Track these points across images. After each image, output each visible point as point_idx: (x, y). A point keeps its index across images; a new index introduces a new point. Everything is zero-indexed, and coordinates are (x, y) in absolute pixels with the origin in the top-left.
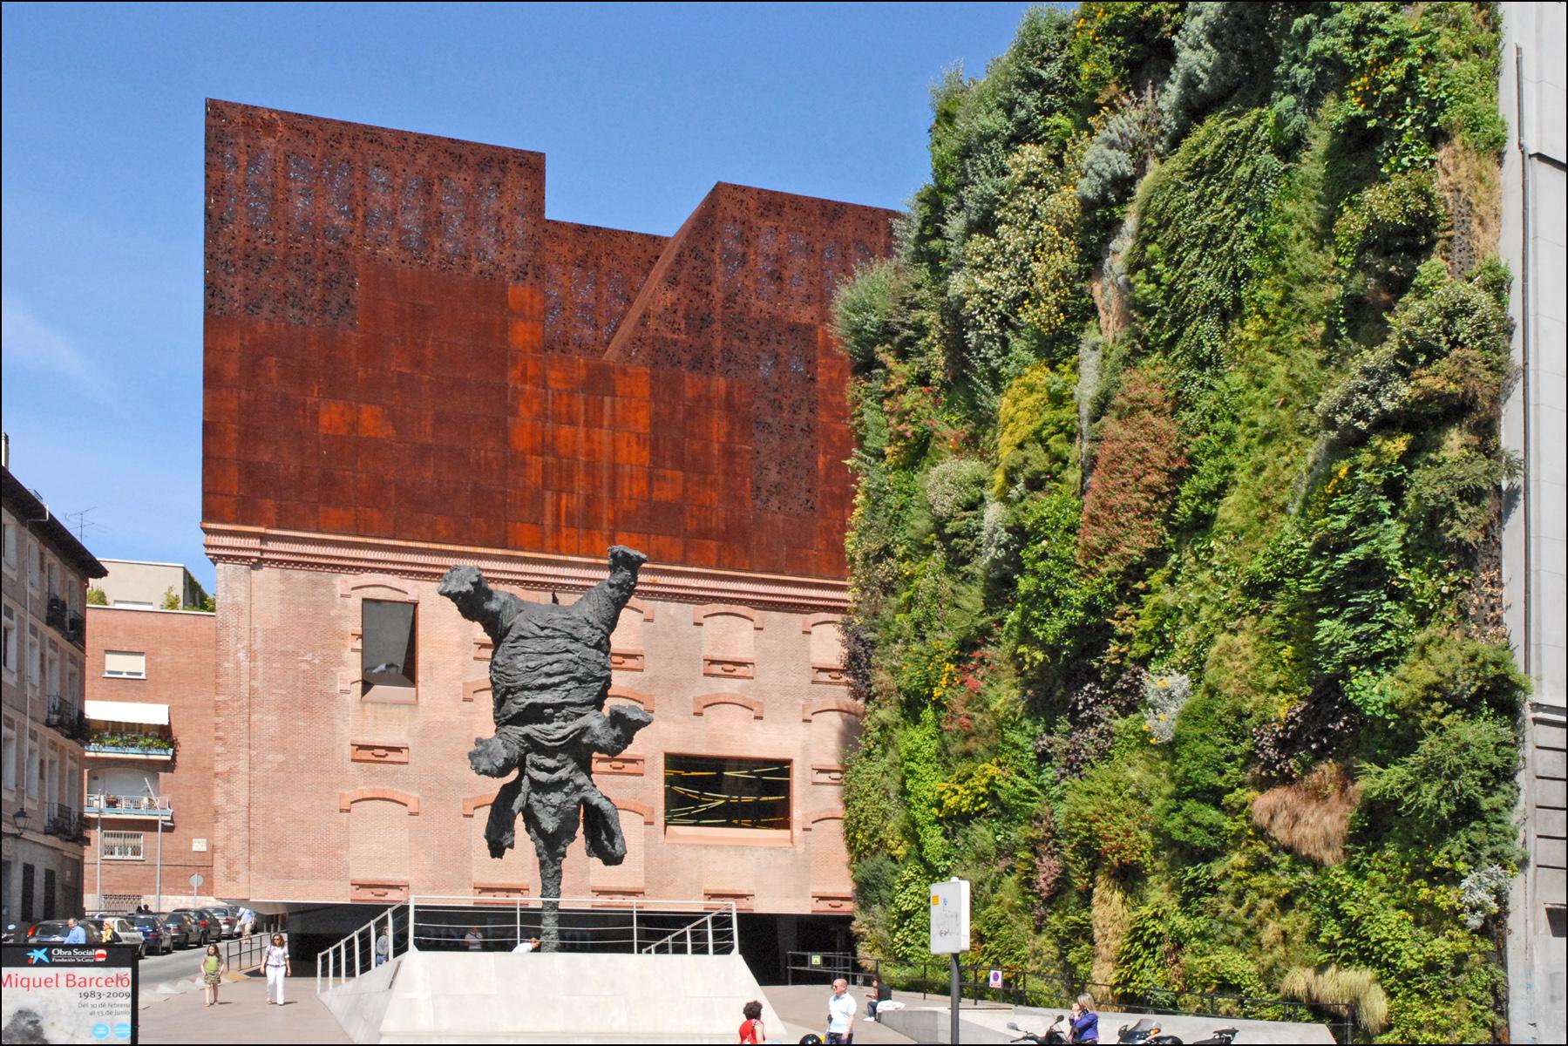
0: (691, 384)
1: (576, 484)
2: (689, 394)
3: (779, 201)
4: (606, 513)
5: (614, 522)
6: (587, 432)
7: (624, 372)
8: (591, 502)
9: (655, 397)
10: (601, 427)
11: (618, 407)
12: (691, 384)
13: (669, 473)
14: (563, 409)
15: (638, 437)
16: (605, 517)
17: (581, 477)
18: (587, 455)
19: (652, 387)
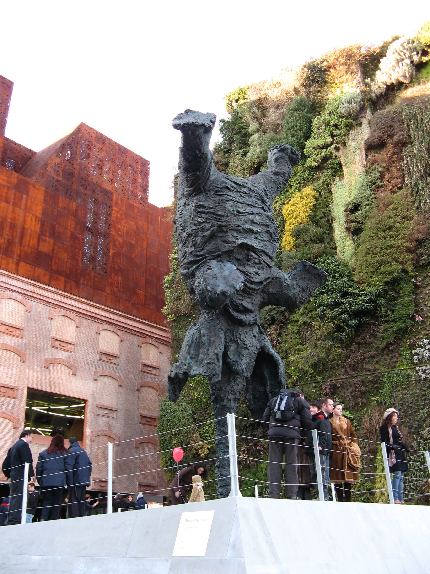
0: (62, 201)
1: (4, 231)
2: (60, 205)
3: (104, 138)
4: (17, 251)
5: (20, 256)
6: (13, 208)
7: (34, 186)
8: (10, 243)
9: (45, 200)
10: (20, 208)
11: (29, 201)
12: (62, 201)
13: (47, 239)
14: (4, 194)
15: (36, 218)
16: (15, 253)
17: (8, 229)
18: (11, 219)
19: (45, 197)
